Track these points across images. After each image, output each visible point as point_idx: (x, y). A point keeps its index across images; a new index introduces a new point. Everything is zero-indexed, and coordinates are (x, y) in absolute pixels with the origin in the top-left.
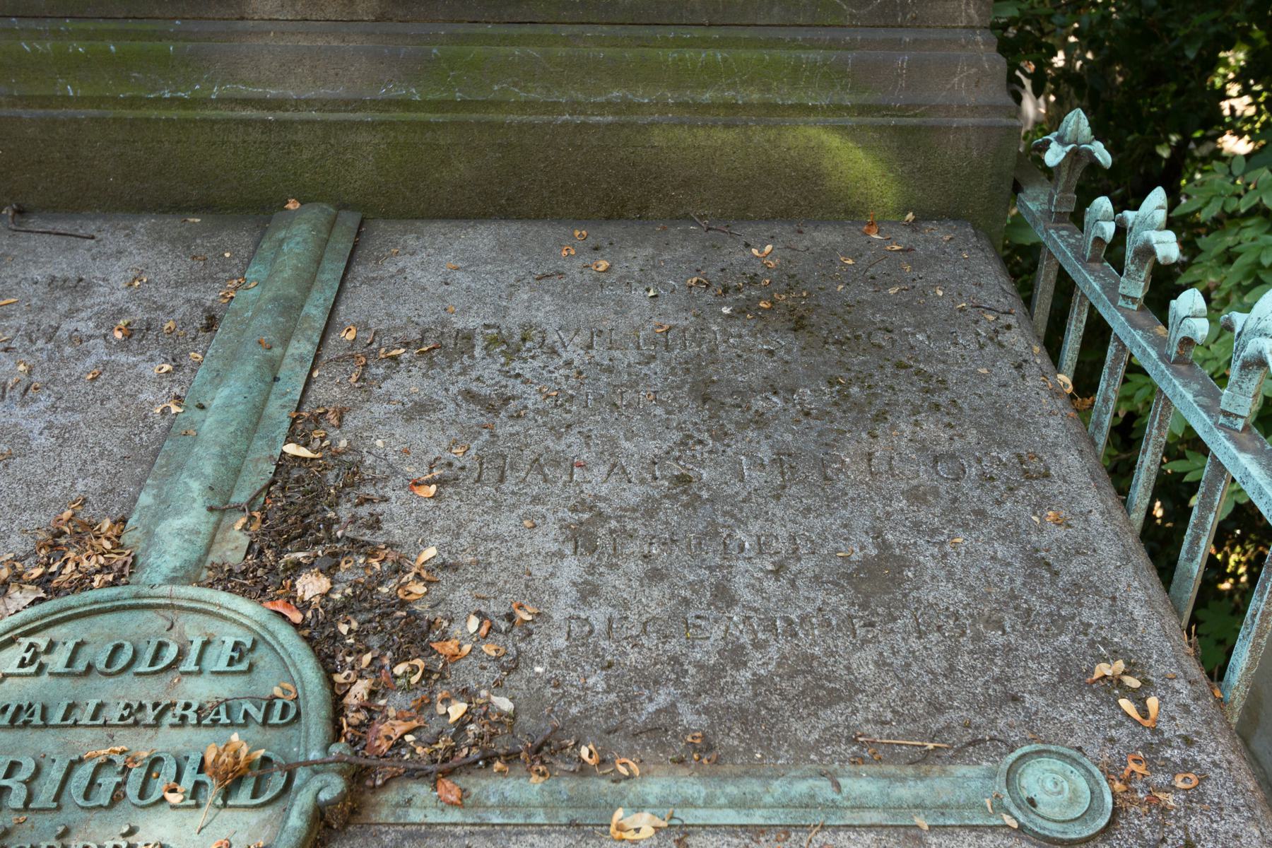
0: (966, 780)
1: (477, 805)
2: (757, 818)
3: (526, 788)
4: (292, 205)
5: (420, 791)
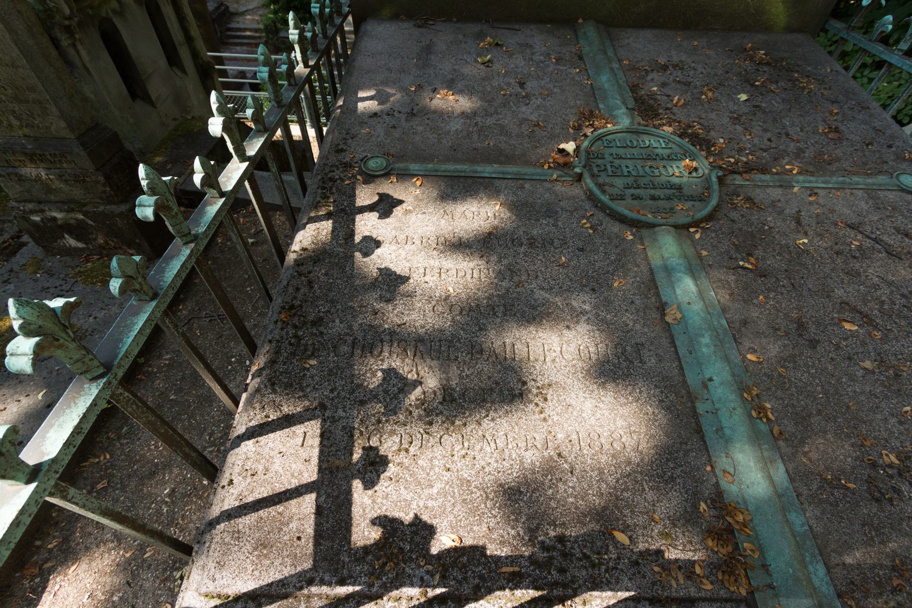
0: (881, 179)
1: (753, 180)
2: (830, 186)
3: (767, 177)
4: (580, 21)
5: (738, 177)
